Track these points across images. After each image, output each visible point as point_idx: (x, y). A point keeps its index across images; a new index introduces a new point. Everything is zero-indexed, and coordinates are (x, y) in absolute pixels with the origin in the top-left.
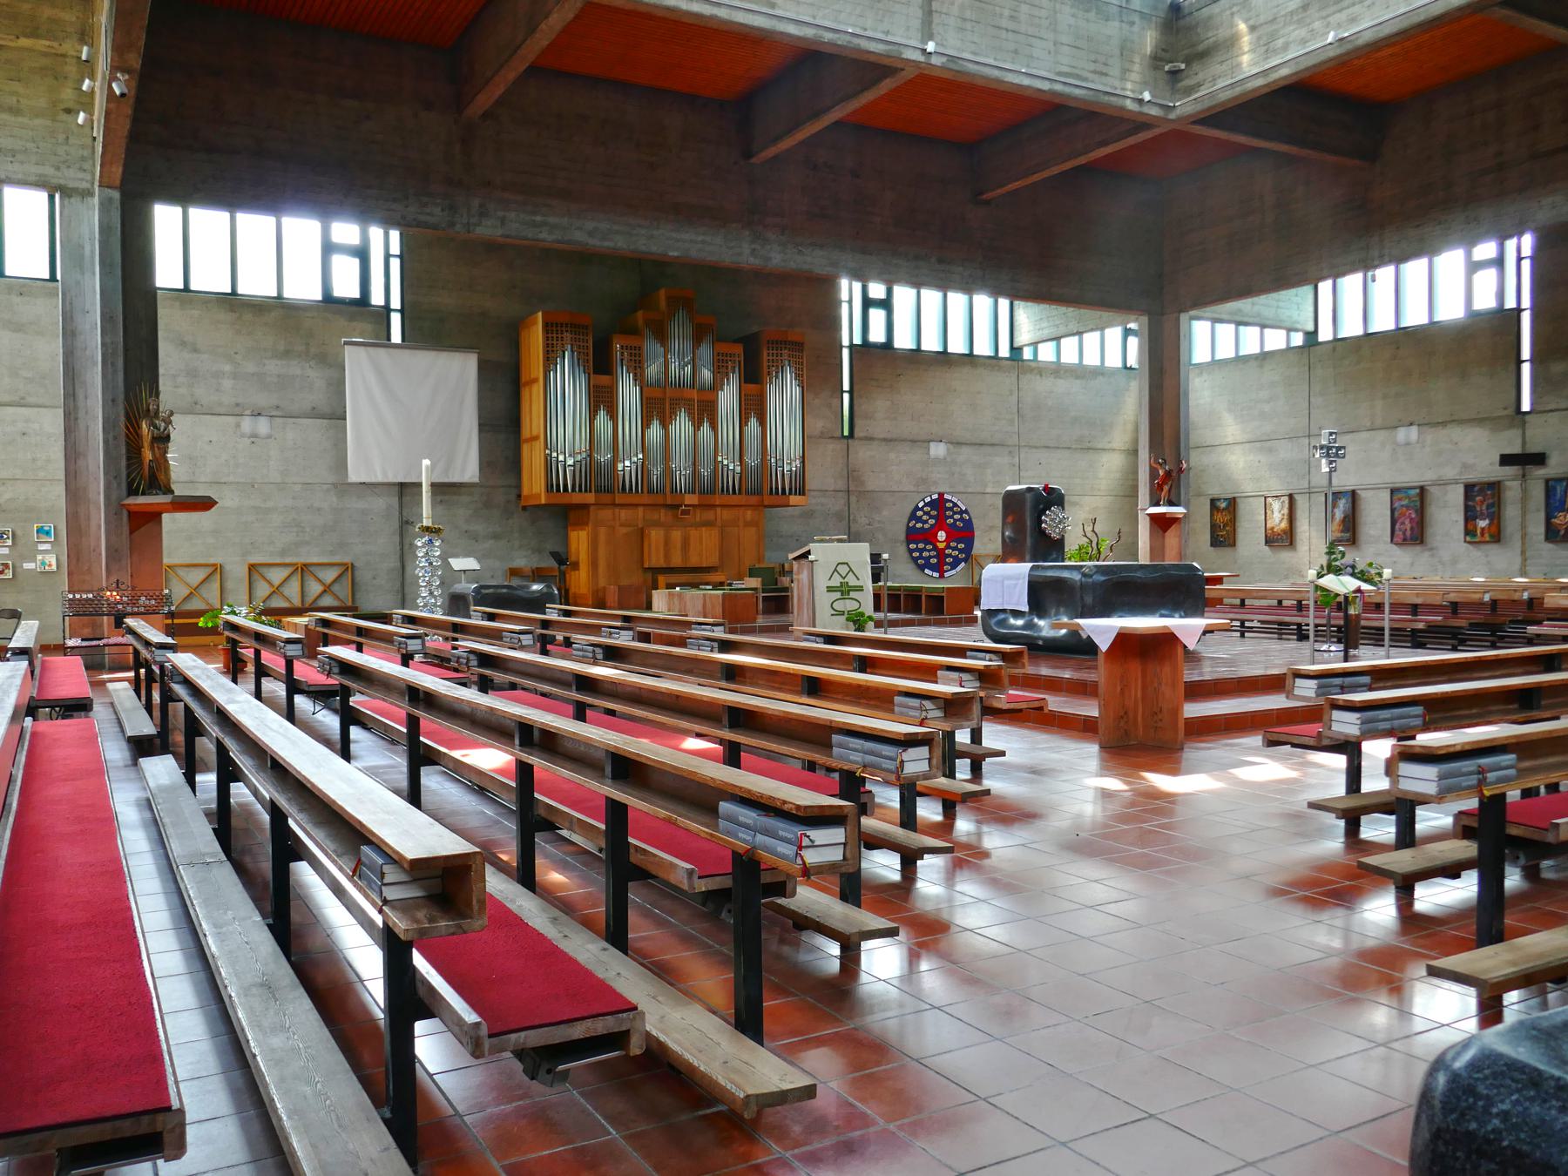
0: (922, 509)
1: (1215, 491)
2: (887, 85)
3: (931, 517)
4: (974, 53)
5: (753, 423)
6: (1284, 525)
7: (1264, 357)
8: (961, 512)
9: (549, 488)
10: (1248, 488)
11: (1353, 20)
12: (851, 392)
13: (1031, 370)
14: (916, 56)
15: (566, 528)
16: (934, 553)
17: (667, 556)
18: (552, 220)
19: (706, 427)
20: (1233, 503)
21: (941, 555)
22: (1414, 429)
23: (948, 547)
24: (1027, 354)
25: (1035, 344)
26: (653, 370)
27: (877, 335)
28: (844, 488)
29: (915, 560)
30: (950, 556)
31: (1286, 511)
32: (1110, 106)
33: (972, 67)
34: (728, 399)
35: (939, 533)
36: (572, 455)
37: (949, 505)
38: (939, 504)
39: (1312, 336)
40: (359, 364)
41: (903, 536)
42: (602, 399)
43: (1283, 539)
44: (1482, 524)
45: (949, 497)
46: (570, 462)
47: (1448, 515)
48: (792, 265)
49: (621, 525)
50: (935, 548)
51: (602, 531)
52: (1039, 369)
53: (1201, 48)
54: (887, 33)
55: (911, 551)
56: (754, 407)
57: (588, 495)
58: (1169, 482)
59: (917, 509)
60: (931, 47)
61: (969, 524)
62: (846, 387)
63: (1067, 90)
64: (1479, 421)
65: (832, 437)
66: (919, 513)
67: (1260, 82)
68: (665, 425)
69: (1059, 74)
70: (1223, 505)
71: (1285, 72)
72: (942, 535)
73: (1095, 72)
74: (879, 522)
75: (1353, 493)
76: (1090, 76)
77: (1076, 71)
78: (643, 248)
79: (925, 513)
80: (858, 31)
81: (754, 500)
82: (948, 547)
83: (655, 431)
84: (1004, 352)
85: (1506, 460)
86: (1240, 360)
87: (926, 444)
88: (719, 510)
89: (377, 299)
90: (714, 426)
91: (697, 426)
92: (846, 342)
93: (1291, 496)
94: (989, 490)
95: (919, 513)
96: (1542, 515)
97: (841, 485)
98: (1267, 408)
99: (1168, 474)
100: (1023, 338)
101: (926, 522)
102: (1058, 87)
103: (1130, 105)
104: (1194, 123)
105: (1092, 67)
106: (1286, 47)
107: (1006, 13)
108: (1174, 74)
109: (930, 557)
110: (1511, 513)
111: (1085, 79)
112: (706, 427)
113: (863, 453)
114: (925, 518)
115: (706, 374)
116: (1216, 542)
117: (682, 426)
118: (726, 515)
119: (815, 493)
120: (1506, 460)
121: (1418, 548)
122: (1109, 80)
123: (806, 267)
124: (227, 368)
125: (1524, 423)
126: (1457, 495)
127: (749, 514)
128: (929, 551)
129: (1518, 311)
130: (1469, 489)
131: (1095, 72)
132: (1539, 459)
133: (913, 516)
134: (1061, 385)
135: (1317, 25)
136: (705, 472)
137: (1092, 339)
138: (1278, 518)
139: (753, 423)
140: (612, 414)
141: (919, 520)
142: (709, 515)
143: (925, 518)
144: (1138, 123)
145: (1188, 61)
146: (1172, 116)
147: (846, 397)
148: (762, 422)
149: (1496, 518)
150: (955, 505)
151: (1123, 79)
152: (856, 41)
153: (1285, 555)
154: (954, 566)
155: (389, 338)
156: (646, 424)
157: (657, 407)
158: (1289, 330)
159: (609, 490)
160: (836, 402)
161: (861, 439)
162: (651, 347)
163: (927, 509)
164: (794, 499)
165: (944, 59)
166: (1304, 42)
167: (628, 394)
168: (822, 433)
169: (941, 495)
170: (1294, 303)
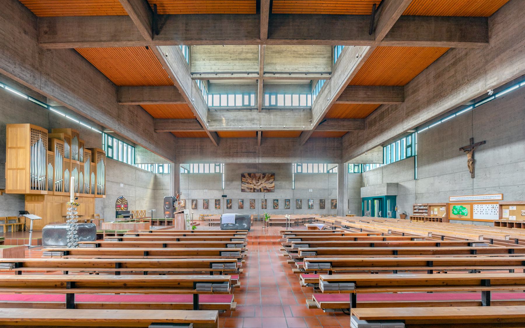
8: (126, 201)
15: (24, 202)
22: (207, 190)
31: (184, 203)
37: (124, 199)
38: (122, 198)
44: (218, 206)
47: (212, 204)
61: (127, 203)
72: (122, 206)
75: (197, 200)
79: (120, 201)
93: (185, 200)
94: (131, 196)
95: (118, 201)
96: (226, 205)
101: (119, 203)
110: (221, 204)
121: (207, 210)
125: (223, 191)
127: (91, 199)
129: (222, 173)
130: (216, 200)
132: (226, 196)
133: (117, 201)
141: (118, 202)
150: (125, 199)
163: (120, 200)
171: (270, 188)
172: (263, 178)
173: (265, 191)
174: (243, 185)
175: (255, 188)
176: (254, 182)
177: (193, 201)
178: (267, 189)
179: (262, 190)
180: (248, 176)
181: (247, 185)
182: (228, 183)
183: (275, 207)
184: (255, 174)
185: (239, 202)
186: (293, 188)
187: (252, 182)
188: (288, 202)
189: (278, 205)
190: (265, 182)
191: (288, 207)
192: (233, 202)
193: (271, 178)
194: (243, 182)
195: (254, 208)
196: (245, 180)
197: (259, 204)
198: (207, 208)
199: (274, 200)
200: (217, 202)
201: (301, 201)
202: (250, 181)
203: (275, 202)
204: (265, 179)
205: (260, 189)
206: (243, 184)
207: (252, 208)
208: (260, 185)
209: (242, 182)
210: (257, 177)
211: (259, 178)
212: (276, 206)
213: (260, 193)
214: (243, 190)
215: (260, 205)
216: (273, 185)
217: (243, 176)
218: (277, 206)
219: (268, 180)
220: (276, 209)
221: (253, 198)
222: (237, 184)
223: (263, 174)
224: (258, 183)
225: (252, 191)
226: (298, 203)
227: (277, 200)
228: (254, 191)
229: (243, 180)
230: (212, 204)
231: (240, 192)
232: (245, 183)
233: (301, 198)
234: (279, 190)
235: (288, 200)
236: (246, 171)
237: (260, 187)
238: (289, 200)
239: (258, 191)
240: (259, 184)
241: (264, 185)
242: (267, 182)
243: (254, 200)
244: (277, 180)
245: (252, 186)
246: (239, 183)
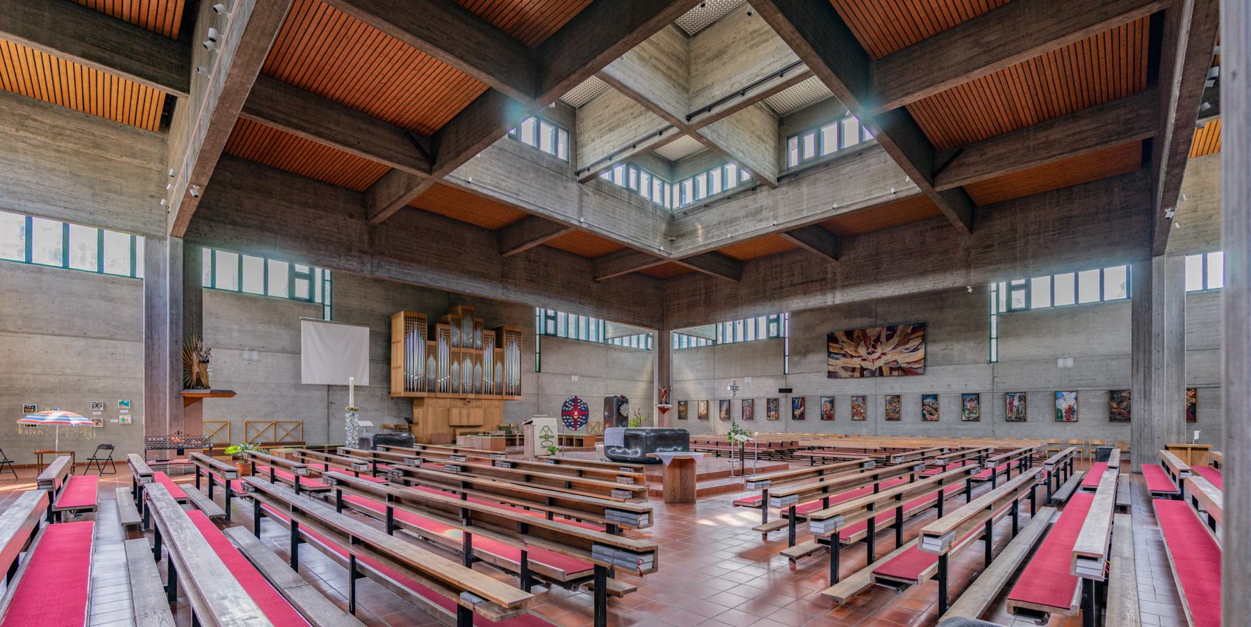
1: (680, 398)
2: (563, 233)
5: (499, 365)
6: (705, 412)
7: (698, 348)
9: (406, 390)
10: (693, 397)
11: (736, 231)
12: (540, 353)
13: (612, 348)
14: (576, 223)
18: (411, 272)
19: (478, 365)
20: (686, 403)
21: (576, 421)
24: (610, 342)
25: (613, 338)
26: (455, 340)
27: (551, 330)
32: (647, 250)
33: (598, 230)
34: (488, 354)
36: (417, 375)
38: (575, 400)
39: (715, 342)
41: (560, 413)
43: (704, 417)
44: (773, 413)
46: (416, 378)
47: (761, 410)
50: (573, 418)
51: (430, 409)
52: (615, 348)
53: (682, 233)
56: (499, 358)
58: (665, 394)
59: (566, 402)
60: (582, 220)
61: (587, 409)
62: (538, 351)
64: (772, 376)
67: (703, 249)
70: (682, 403)
71: (712, 246)
72: (576, 413)
78: (455, 288)
81: (499, 397)
83: (456, 365)
84: (601, 340)
85: (781, 391)
86: (689, 349)
90: (482, 366)
91: (474, 365)
92: (538, 333)
98: (699, 367)
99: (665, 391)
100: (610, 334)
102: (630, 241)
103: (657, 252)
104: (681, 260)
106: (713, 237)
108: (672, 241)
110: (782, 409)
112: (478, 365)
113: (544, 378)
116: (680, 417)
117: (468, 364)
118: (487, 403)
120: (781, 391)
126: (764, 402)
127: (497, 403)
132: (790, 391)
133: (564, 405)
134: (623, 355)
135: (724, 230)
136: (478, 384)
137: (634, 338)
138: (703, 410)
139: (499, 365)
140: (436, 358)
141: (567, 407)
142: (479, 403)
144: (659, 259)
145: (677, 237)
146: (671, 257)
147: (538, 355)
149: (777, 411)
153: (705, 423)
154: (581, 426)
156: (451, 363)
157: (455, 357)
158: (707, 339)
159: (433, 391)
160: (533, 357)
164: (516, 397)
166: (719, 236)
167: (443, 349)
169: (576, 397)
170: (709, 330)
171: (908, 363)
172: (889, 338)
173: (895, 373)
174: (832, 361)
175: (864, 366)
176: (862, 351)
177: (721, 402)
178: (900, 369)
179: (886, 370)
180: (844, 339)
181: (842, 362)
182: (796, 359)
183: (928, 416)
184: (863, 331)
185: (823, 403)
186: (994, 359)
187: (856, 351)
188: (971, 400)
189: (936, 410)
190: (893, 349)
191: (972, 415)
192: (808, 404)
193: (912, 337)
194: (832, 355)
195: (864, 419)
196: (837, 348)
197: (876, 406)
198: (751, 417)
199: (925, 397)
200: (772, 405)
201: (1023, 398)
202: (850, 350)
203: (929, 401)
204: (895, 340)
205: (880, 368)
206: (833, 358)
207: (856, 418)
208: (879, 357)
209: (829, 353)
210: (869, 338)
211: (878, 340)
212: (931, 414)
213: (879, 379)
214: (832, 375)
215: (881, 410)
216: (920, 354)
217: (832, 338)
218: (934, 412)
219: (905, 340)
220: (932, 420)
221: (861, 393)
222: (818, 359)
223: (889, 329)
224: (874, 352)
225: (857, 374)
226: (1011, 404)
227: (935, 397)
228: (862, 376)
229: (831, 350)
230: (761, 410)
231: (824, 379)
232: (837, 356)
233: (1024, 387)
234: (942, 367)
235: (973, 397)
236: (839, 325)
237: (880, 363)
238: (978, 394)
239: (873, 374)
240: (875, 356)
241: (890, 357)
242: (900, 348)
243: (864, 398)
244: (934, 341)
245: (856, 362)
246: (823, 356)
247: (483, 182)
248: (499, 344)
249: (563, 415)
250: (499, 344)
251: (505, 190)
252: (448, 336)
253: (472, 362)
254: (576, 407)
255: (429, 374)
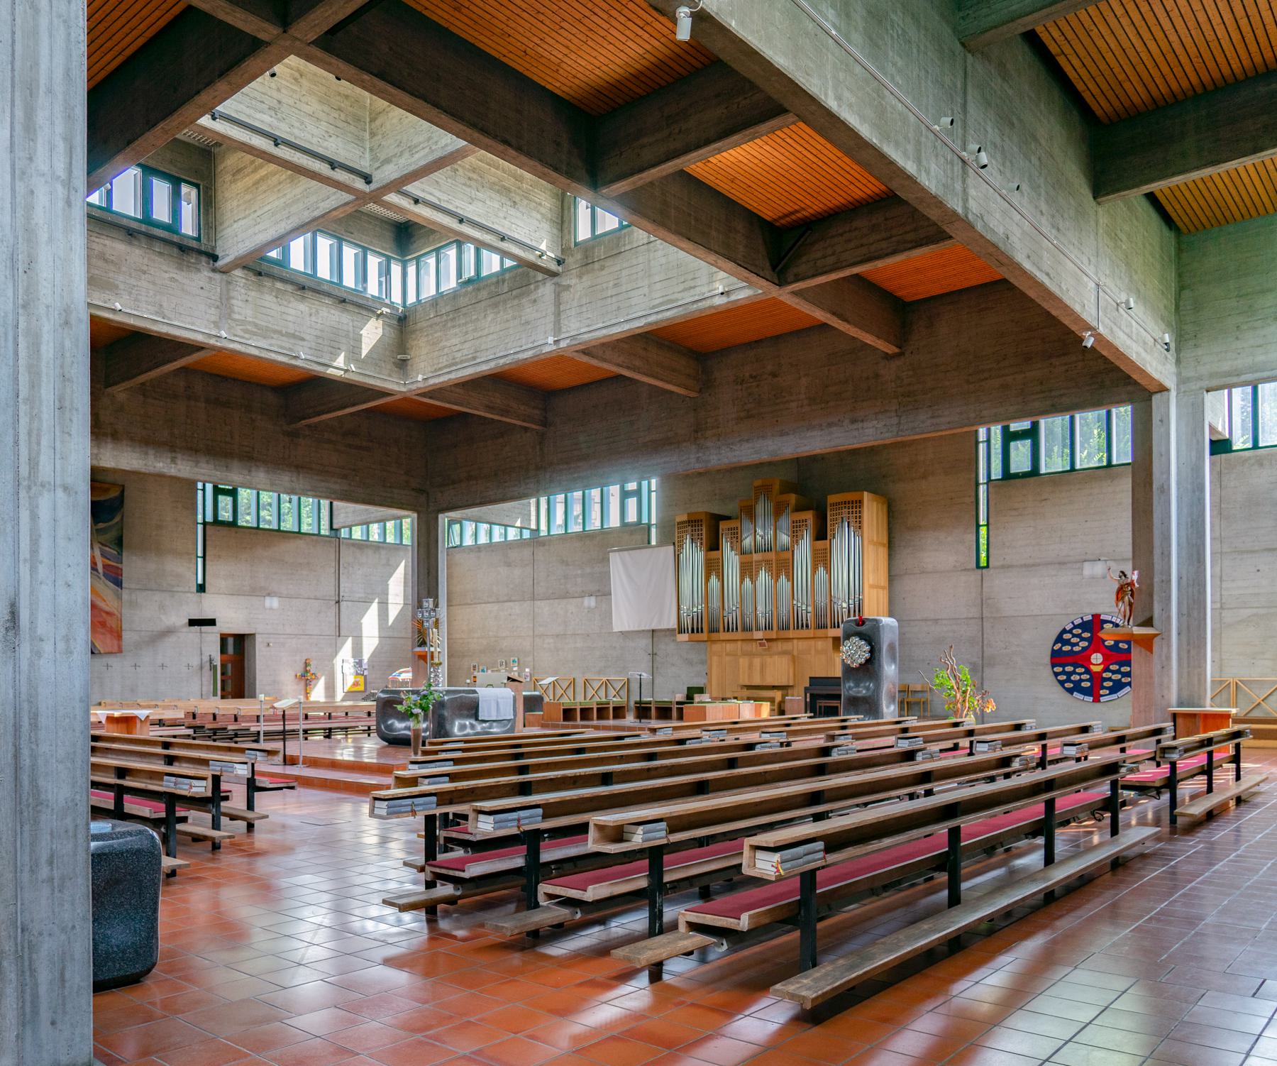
0: (1070, 631)
3: (1083, 639)
4: (588, 326)
5: (821, 570)
16: (1087, 676)
17: (750, 676)
19: (783, 578)
21: (1097, 680)
23: (1106, 669)
26: (748, 542)
28: (978, 615)
29: (1062, 683)
30: (1109, 679)
33: (586, 337)
35: (1094, 656)
40: (617, 562)
41: (1047, 660)
42: (713, 567)
45: (1109, 618)
48: (726, 461)
49: (727, 655)
50: (1088, 671)
51: (715, 659)
54: (533, 342)
55: (1056, 674)
56: (822, 559)
57: (700, 634)
59: (1064, 631)
63: (660, 316)
65: (965, 570)
66: (1067, 636)
68: (753, 581)
69: (654, 307)
72: (1097, 658)
73: (684, 290)
74: (1018, 645)
76: (679, 296)
77: (665, 299)
79: (1074, 636)
80: (518, 349)
82: (1106, 669)
87: (1078, 565)
88: (795, 641)
89: (645, 520)
97: (974, 612)
101: (1077, 644)
102: (652, 319)
103: (719, 301)
105: (682, 287)
107: (611, 284)
109: (1081, 681)
111: (677, 300)
112: (783, 578)
113: (997, 583)
114: (1074, 640)
115: (784, 539)
118: (801, 645)
119: (944, 622)
122: (698, 290)
123: (735, 460)
124: (579, 572)
128: (1080, 674)
131: (684, 290)
133: (1059, 639)
136: (784, 611)
141: (1067, 642)
143: (1074, 640)
148: (828, 570)
151: (711, 282)
152: (516, 357)
154: (1113, 690)
155: (649, 542)
157: (747, 570)
161: (995, 568)
162: (747, 525)
163: (1078, 631)
165: (568, 341)
167: (731, 559)
168: (955, 566)
247: (440, 369)
248: (821, 534)
249: (1053, 666)
250: (821, 534)
251: (462, 362)
252: (736, 537)
253: (769, 570)
254: (1096, 644)
255: (712, 603)
